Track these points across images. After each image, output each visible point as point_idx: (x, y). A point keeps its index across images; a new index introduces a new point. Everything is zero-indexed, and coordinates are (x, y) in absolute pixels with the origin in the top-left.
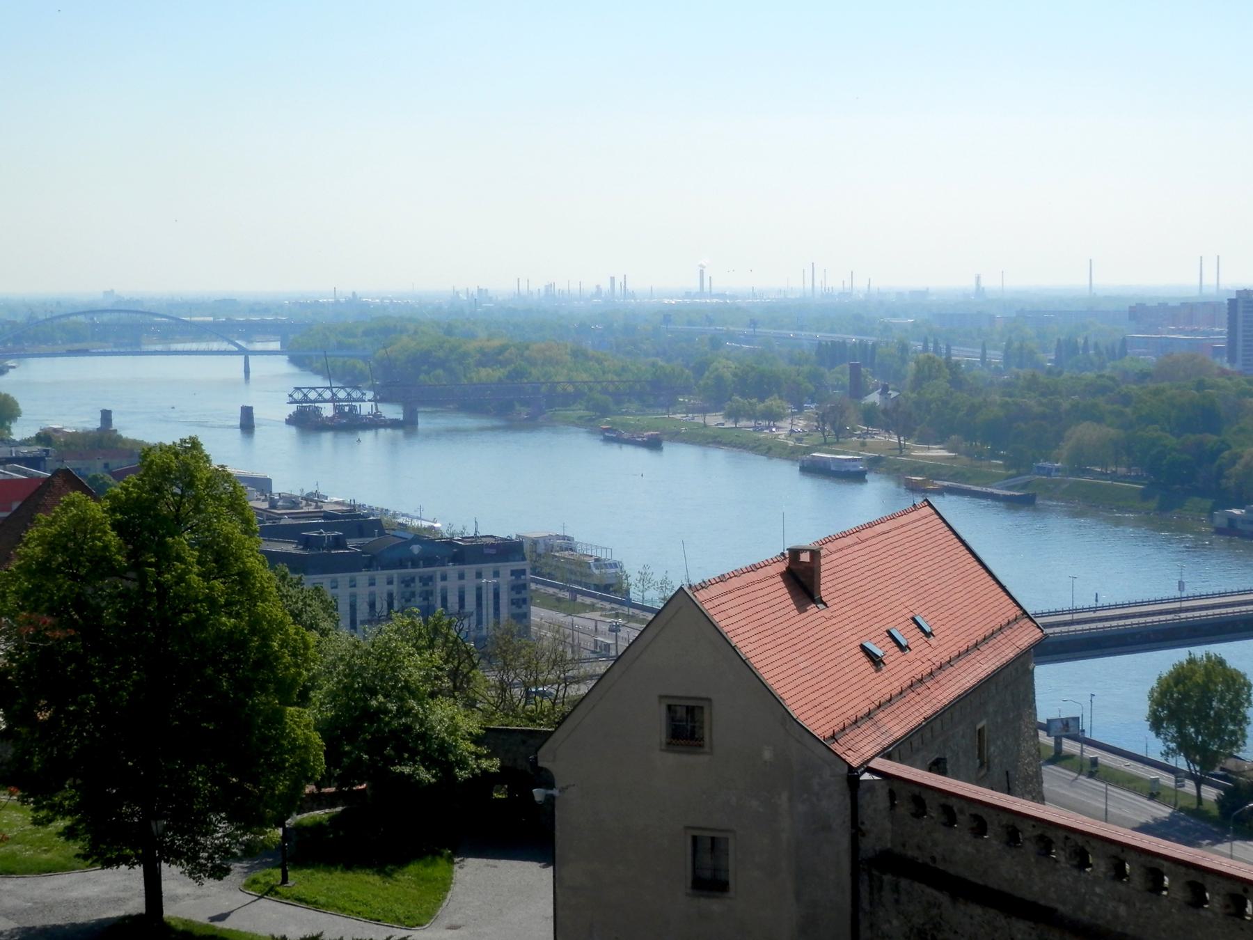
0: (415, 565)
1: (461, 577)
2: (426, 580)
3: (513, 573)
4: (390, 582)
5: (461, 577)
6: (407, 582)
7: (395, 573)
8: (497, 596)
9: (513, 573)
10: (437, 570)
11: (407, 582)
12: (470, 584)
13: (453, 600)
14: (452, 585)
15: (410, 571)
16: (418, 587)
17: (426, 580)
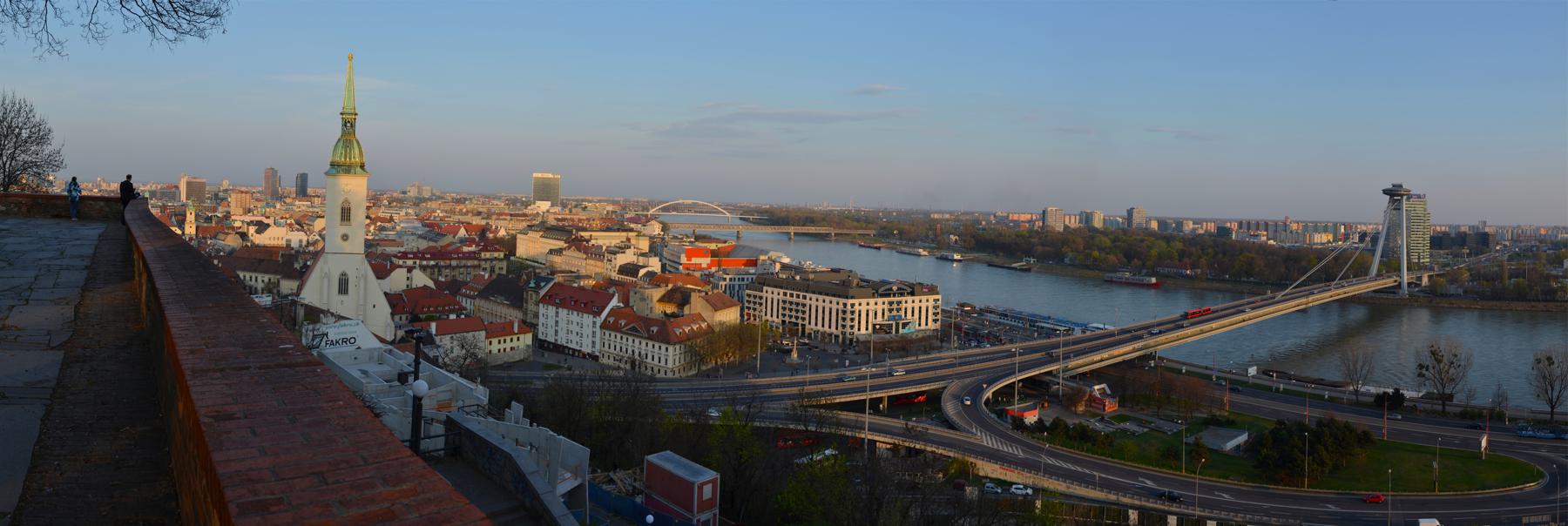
0: (894, 296)
1: (913, 302)
2: (899, 303)
3: (934, 300)
4: (884, 303)
5: (913, 302)
6: (891, 303)
7: (886, 300)
8: (927, 311)
9: (934, 300)
10: (903, 299)
11: (891, 303)
12: (917, 305)
13: (909, 312)
14: (909, 306)
15: (892, 299)
16: (895, 306)
17: (899, 303)
